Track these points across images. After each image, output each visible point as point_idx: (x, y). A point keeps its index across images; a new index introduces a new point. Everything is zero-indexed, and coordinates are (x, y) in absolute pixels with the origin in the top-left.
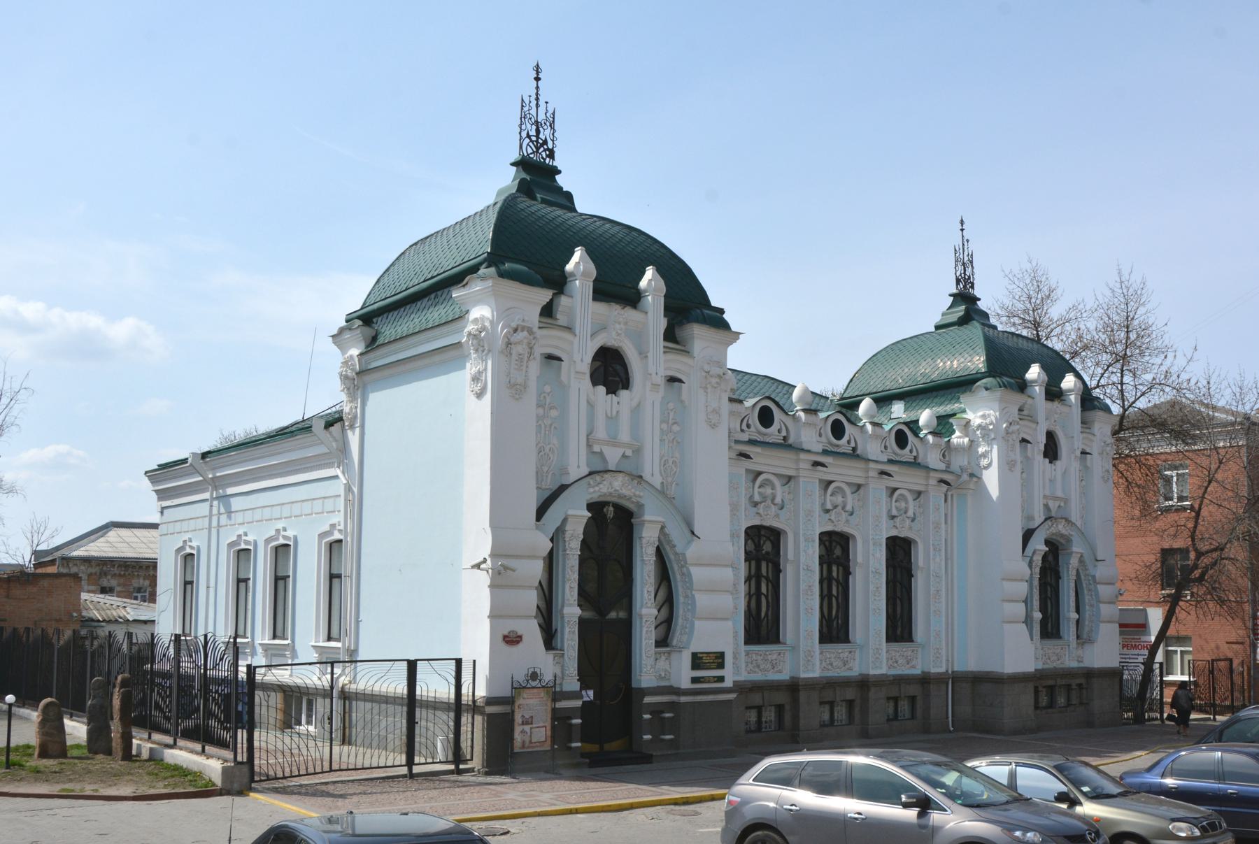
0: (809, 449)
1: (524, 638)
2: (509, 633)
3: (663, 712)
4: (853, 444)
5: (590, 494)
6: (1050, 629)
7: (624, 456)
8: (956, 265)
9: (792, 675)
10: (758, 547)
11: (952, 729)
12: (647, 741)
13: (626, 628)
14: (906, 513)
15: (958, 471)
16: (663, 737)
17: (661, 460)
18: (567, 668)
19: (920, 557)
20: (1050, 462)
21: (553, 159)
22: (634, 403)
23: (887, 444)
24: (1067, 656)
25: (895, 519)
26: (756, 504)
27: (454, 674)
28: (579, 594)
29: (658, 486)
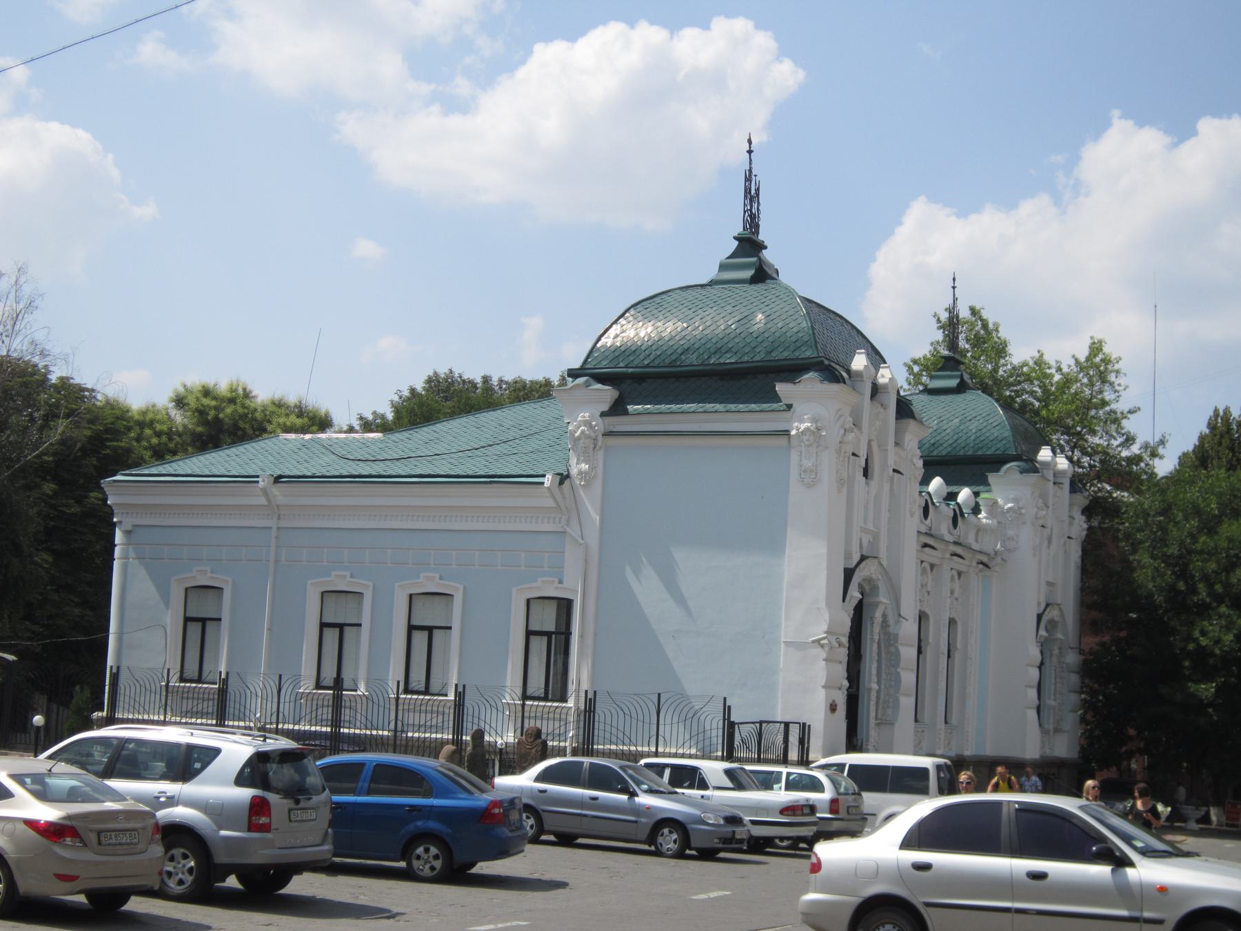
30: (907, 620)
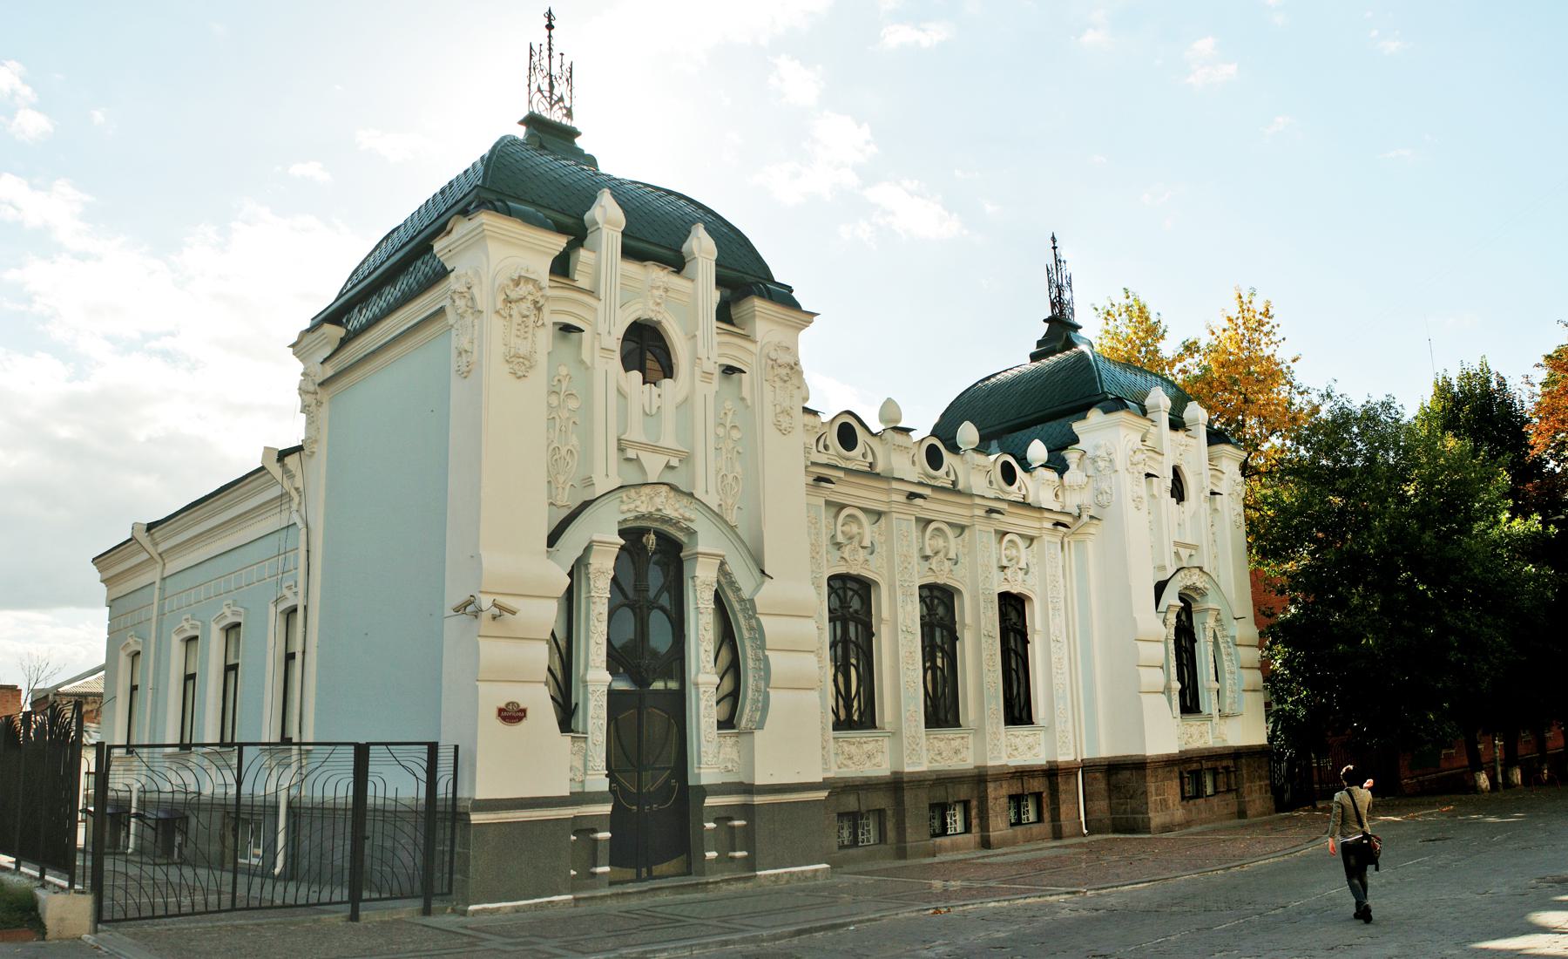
0: (902, 477)
2: (508, 704)
3: (731, 819)
4: (952, 477)
6: (1190, 704)
7: (669, 467)
8: (1050, 287)
9: (893, 770)
10: (844, 603)
11: (1085, 831)
12: (711, 860)
13: (677, 705)
14: (1017, 563)
15: (1076, 512)
16: (731, 854)
17: (717, 475)
18: (591, 759)
19: (1035, 618)
20: (1178, 504)
21: (572, 119)
22: (680, 398)
23: (993, 479)
24: (1210, 734)
25: (1006, 570)
26: (839, 546)
27: (425, 765)
28: (609, 655)
29: (716, 509)
30: (772, 578)
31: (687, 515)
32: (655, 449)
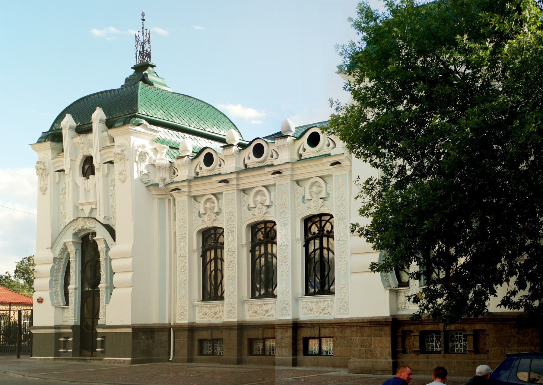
1: (44, 300)
5: (74, 230)
12: (99, 352)
31: (91, 226)
32: (86, 204)
